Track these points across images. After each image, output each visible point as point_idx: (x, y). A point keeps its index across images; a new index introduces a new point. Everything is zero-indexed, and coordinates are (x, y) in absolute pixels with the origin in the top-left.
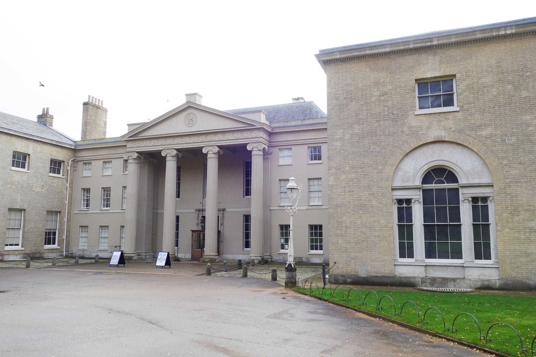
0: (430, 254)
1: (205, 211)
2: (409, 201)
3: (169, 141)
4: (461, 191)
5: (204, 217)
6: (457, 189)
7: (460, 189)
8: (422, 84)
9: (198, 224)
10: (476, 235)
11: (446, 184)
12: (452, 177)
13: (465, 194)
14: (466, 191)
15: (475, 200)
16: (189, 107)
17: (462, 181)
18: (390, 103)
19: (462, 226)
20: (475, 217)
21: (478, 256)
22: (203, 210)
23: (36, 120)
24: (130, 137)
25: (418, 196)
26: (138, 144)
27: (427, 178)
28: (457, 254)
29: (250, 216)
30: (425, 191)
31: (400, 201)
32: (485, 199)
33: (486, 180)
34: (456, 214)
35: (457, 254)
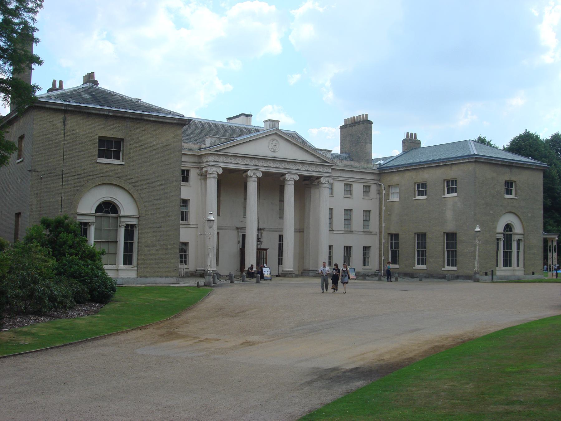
1: (245, 229)
3: (256, 162)
4: (513, 236)
5: (244, 236)
6: (511, 235)
7: (513, 235)
9: (239, 242)
11: (509, 232)
14: (516, 236)
16: (276, 133)
18: (496, 190)
19: (512, 252)
22: (244, 228)
24: (215, 151)
25: (501, 236)
29: (282, 236)
30: (504, 234)
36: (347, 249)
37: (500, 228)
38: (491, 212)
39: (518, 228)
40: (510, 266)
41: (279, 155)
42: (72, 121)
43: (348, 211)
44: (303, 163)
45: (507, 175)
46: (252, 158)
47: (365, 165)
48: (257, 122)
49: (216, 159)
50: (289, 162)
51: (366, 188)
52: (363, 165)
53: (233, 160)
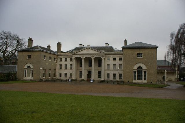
0: (138, 79)
2: (135, 71)
8: (138, 54)
10: (144, 77)
12: (141, 68)
13: (143, 71)
15: (144, 72)
17: (143, 69)
20: (144, 74)
21: (144, 80)
23: (46, 47)
25: (137, 71)
26: (75, 55)
27: (138, 68)
28: (142, 79)
30: (138, 70)
31: (134, 71)
32: (146, 71)
33: (146, 69)
34: (142, 74)
35: (142, 79)
36: (114, 75)
37: (136, 67)
38: (130, 63)
39: (144, 67)
40: (135, 79)
41: (89, 53)
42: (23, 53)
43: (114, 65)
44: (96, 54)
45: (139, 51)
46: (82, 54)
47: (114, 52)
48: (85, 46)
49: (74, 55)
50: (92, 54)
51: (121, 59)
52: (114, 52)
53: (78, 55)
